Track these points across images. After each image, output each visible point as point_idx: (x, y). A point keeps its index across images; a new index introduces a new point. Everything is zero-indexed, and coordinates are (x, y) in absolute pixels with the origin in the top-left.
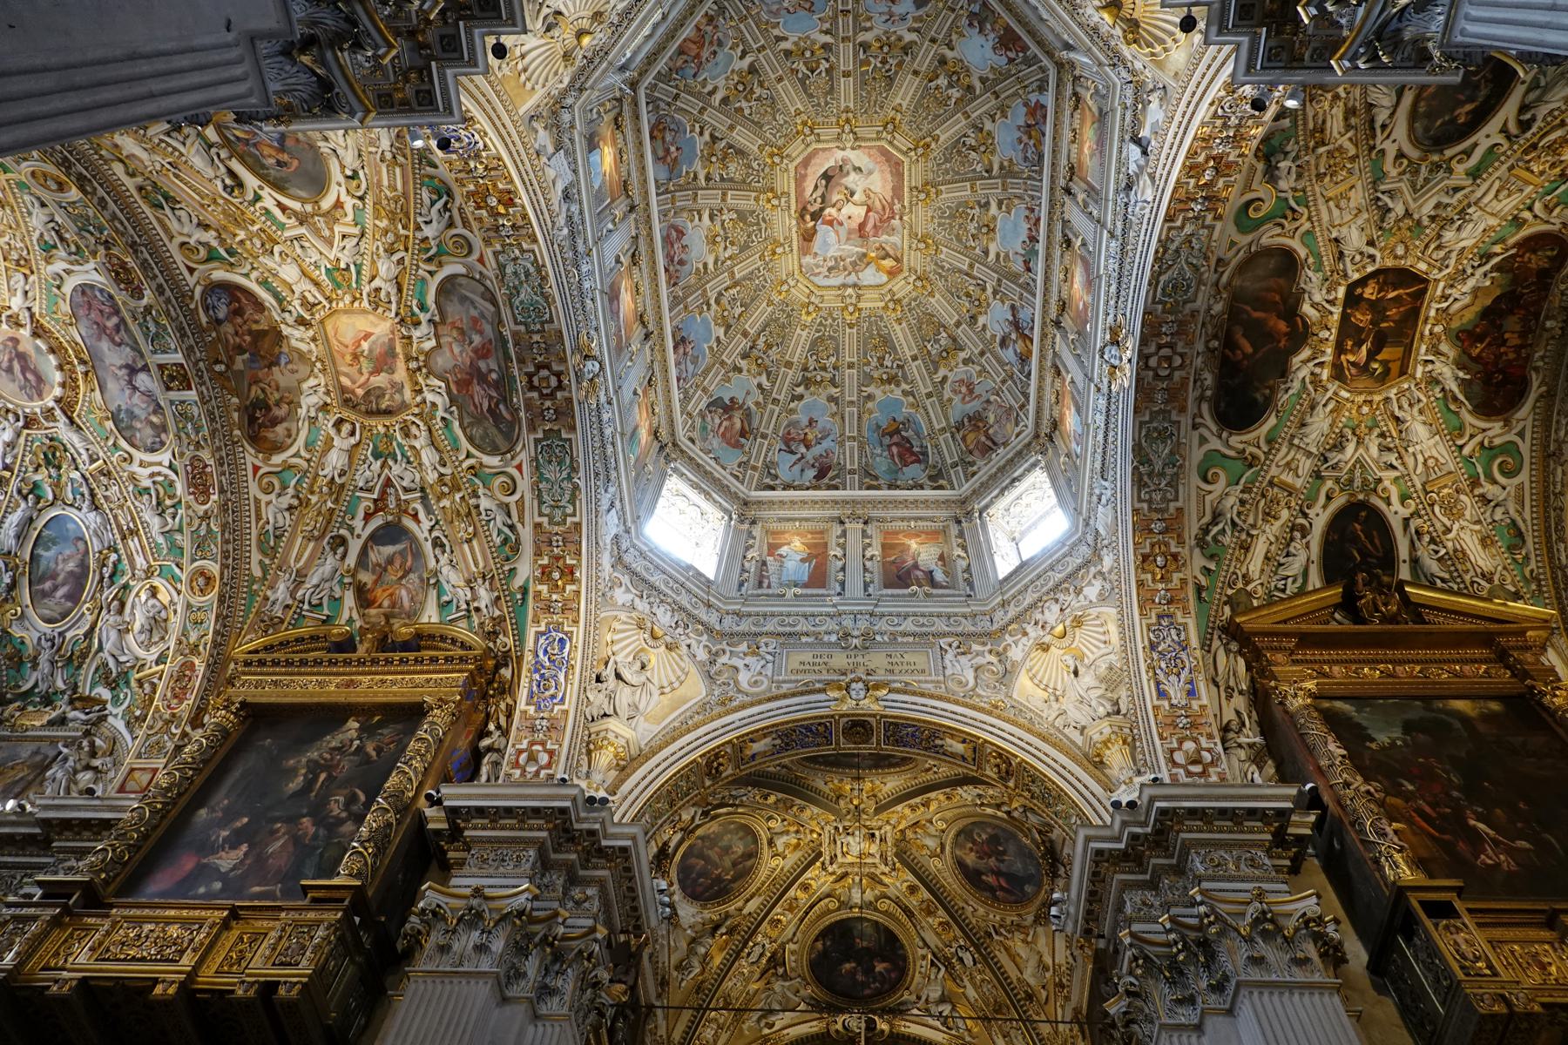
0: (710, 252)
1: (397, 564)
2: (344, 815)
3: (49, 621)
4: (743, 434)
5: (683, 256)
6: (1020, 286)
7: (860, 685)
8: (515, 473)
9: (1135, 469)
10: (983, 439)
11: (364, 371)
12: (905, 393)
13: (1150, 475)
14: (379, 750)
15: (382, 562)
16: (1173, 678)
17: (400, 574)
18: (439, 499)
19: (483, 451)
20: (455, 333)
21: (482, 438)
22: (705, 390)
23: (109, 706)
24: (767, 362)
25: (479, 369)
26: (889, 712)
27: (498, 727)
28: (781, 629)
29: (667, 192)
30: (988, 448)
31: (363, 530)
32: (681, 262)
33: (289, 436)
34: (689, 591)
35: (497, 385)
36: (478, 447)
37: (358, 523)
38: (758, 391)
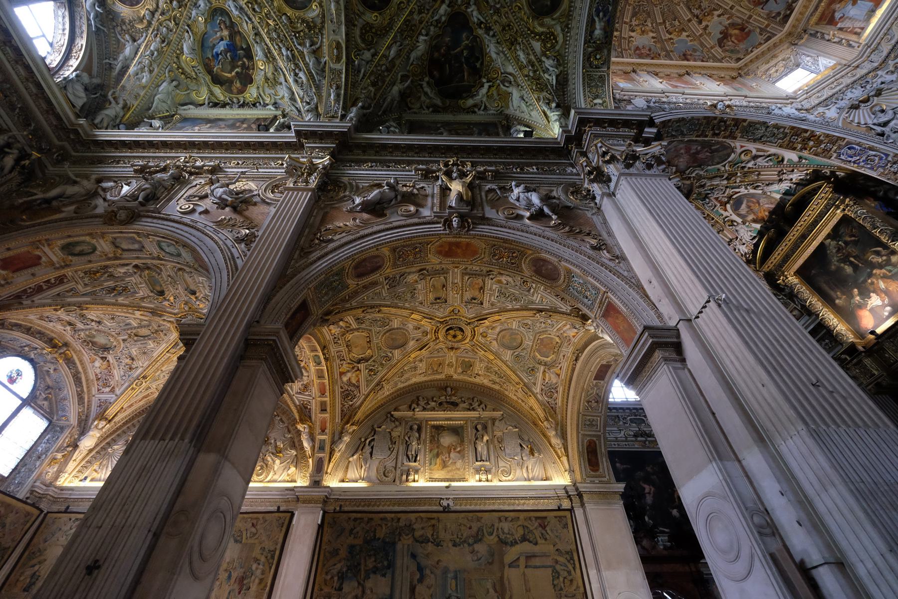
0: (647, 34)
1: (752, 205)
4: (742, 29)
5: (647, 48)
8: (743, 149)
14: (854, 236)
15: (747, 210)
18: (735, 182)
19: (726, 160)
22: (712, 48)
24: (707, 10)
25: (693, 153)
27: (874, 187)
29: (621, 52)
32: (650, 50)
34: (842, 77)
35: (703, 148)
36: (722, 162)
38: (722, 18)
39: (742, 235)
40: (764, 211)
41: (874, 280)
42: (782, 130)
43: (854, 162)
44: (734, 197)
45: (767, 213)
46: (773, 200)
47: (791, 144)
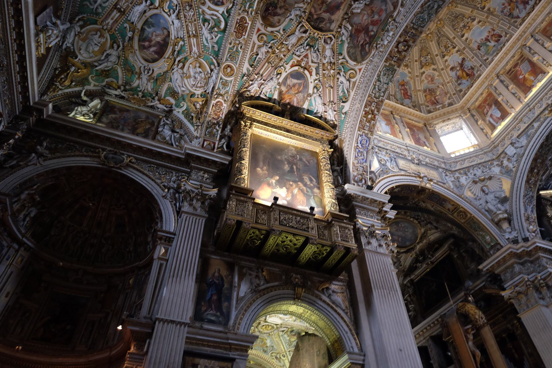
1: (296, 88)
2: (312, 185)
3: (146, 60)
6: (473, 53)
7: (426, 178)
8: (358, 71)
9: (544, 142)
10: (433, 99)
11: (322, 9)
12: (410, 73)
13: (546, 145)
14: (309, 163)
15: (291, 85)
16: (528, 206)
17: (296, 92)
20: (369, 12)
21: (353, 54)
23: (174, 106)
26: (434, 189)
28: (391, 149)
30: (435, 103)
31: (289, 69)
33: (279, 22)
37: (288, 67)
39: (269, 84)
40: (290, 99)
41: (294, 186)
42: (382, 94)
43: (358, 146)
44: (306, 72)
45: (288, 101)
46: (302, 103)
47: (370, 103)
